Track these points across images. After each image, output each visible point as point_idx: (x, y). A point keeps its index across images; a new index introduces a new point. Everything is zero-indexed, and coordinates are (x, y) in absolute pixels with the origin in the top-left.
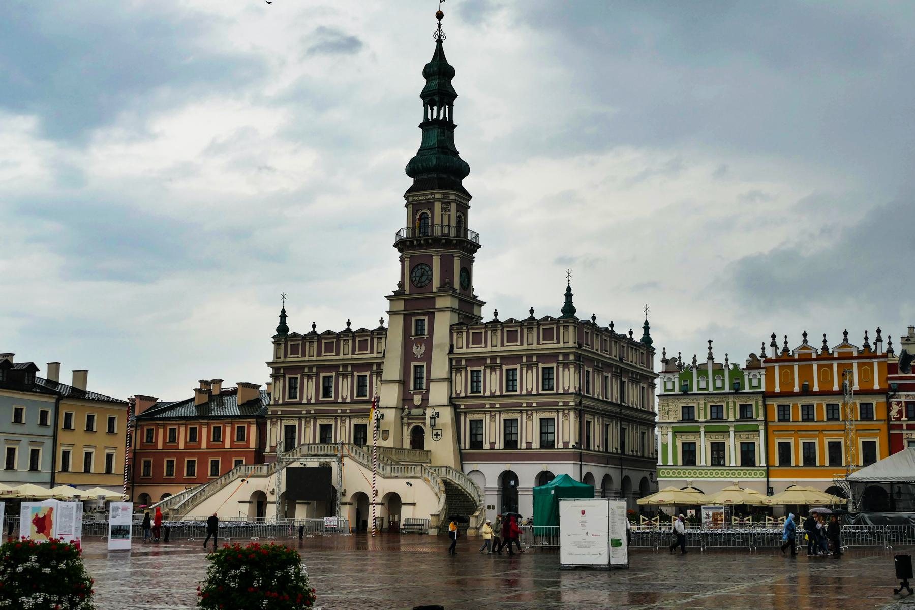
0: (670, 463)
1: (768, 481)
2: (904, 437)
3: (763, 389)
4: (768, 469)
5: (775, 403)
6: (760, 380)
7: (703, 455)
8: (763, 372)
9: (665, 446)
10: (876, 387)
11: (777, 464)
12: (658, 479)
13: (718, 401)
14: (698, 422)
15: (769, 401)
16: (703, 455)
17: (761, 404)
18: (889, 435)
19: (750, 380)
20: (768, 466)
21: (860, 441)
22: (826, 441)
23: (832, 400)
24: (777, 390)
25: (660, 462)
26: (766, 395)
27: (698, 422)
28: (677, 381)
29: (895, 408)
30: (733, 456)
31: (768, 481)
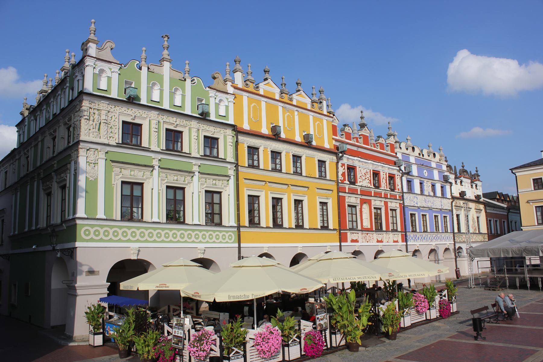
0: (101, 214)
1: (239, 247)
2: (346, 200)
3: (231, 122)
4: (239, 231)
5: (246, 141)
6: (227, 107)
7: (154, 206)
8: (231, 98)
9: (92, 184)
10: (327, 146)
11: (247, 224)
12: (78, 244)
13: (174, 123)
14: (147, 150)
15: (241, 138)
16: (154, 206)
17: (230, 140)
18: (339, 197)
19: (217, 105)
20: (239, 227)
21: (318, 200)
22: (293, 198)
23: (298, 151)
24: (246, 126)
25: (81, 212)
26: (237, 131)
27: (147, 150)
28: (115, 78)
29: (341, 170)
30: (195, 209)
31: (239, 247)
